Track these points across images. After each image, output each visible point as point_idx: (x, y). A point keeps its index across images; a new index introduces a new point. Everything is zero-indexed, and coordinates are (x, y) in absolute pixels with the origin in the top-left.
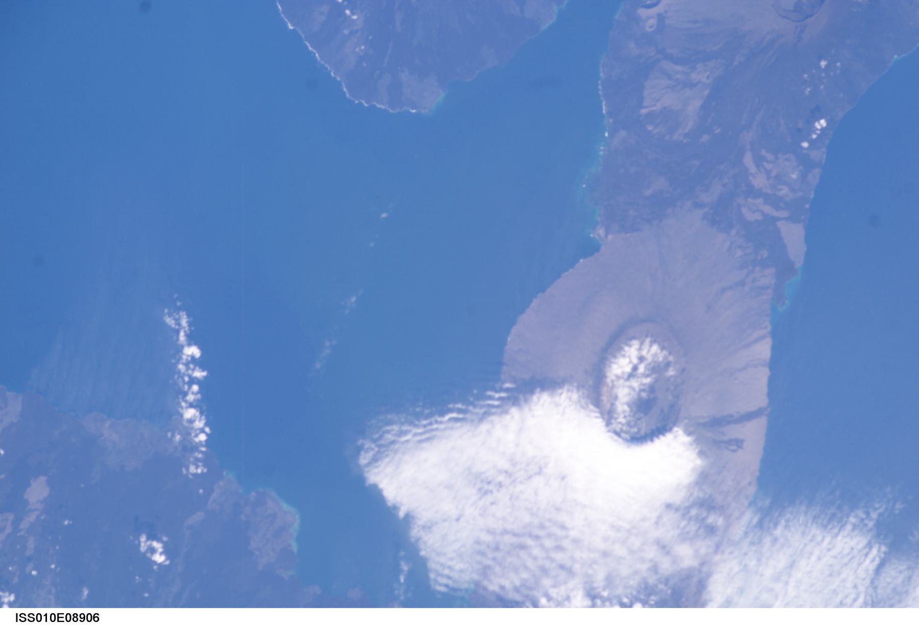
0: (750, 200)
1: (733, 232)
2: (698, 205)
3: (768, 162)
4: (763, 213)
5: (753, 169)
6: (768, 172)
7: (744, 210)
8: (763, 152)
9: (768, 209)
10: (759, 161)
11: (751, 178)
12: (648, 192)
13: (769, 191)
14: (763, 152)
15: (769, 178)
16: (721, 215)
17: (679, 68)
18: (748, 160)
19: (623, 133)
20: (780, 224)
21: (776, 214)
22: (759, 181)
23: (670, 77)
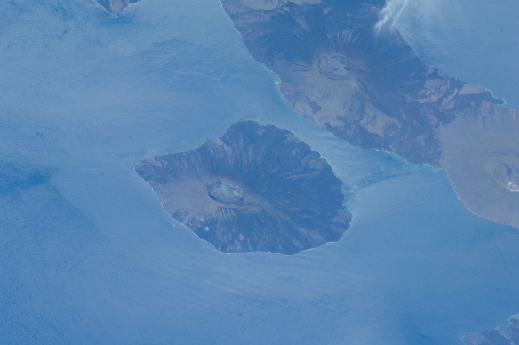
0: (442, 105)
1: (456, 115)
2: (437, 126)
3: (426, 92)
4: (453, 100)
5: (427, 100)
6: (431, 93)
7: (447, 108)
8: (420, 94)
9: (450, 98)
10: (424, 96)
11: (431, 102)
12: (423, 143)
13: (441, 95)
14: (420, 94)
15: (435, 94)
16: (445, 118)
17: (365, 118)
18: (422, 101)
19: (391, 146)
20: (460, 93)
21: (455, 94)
22: (435, 98)
23: (368, 123)
